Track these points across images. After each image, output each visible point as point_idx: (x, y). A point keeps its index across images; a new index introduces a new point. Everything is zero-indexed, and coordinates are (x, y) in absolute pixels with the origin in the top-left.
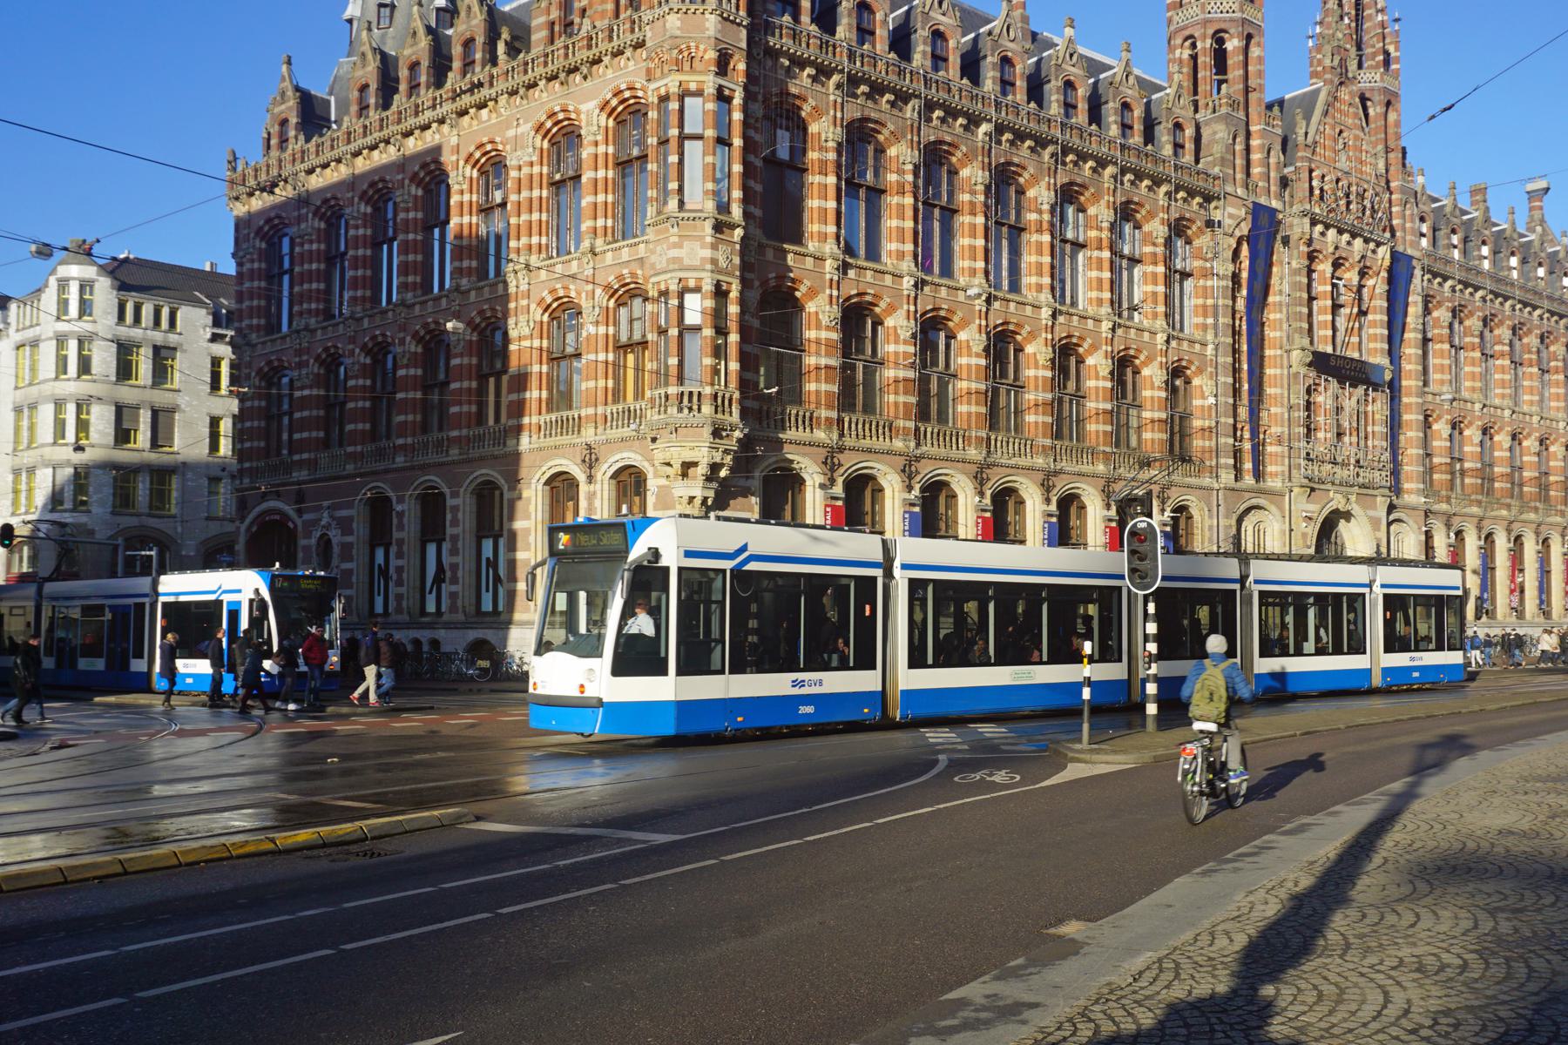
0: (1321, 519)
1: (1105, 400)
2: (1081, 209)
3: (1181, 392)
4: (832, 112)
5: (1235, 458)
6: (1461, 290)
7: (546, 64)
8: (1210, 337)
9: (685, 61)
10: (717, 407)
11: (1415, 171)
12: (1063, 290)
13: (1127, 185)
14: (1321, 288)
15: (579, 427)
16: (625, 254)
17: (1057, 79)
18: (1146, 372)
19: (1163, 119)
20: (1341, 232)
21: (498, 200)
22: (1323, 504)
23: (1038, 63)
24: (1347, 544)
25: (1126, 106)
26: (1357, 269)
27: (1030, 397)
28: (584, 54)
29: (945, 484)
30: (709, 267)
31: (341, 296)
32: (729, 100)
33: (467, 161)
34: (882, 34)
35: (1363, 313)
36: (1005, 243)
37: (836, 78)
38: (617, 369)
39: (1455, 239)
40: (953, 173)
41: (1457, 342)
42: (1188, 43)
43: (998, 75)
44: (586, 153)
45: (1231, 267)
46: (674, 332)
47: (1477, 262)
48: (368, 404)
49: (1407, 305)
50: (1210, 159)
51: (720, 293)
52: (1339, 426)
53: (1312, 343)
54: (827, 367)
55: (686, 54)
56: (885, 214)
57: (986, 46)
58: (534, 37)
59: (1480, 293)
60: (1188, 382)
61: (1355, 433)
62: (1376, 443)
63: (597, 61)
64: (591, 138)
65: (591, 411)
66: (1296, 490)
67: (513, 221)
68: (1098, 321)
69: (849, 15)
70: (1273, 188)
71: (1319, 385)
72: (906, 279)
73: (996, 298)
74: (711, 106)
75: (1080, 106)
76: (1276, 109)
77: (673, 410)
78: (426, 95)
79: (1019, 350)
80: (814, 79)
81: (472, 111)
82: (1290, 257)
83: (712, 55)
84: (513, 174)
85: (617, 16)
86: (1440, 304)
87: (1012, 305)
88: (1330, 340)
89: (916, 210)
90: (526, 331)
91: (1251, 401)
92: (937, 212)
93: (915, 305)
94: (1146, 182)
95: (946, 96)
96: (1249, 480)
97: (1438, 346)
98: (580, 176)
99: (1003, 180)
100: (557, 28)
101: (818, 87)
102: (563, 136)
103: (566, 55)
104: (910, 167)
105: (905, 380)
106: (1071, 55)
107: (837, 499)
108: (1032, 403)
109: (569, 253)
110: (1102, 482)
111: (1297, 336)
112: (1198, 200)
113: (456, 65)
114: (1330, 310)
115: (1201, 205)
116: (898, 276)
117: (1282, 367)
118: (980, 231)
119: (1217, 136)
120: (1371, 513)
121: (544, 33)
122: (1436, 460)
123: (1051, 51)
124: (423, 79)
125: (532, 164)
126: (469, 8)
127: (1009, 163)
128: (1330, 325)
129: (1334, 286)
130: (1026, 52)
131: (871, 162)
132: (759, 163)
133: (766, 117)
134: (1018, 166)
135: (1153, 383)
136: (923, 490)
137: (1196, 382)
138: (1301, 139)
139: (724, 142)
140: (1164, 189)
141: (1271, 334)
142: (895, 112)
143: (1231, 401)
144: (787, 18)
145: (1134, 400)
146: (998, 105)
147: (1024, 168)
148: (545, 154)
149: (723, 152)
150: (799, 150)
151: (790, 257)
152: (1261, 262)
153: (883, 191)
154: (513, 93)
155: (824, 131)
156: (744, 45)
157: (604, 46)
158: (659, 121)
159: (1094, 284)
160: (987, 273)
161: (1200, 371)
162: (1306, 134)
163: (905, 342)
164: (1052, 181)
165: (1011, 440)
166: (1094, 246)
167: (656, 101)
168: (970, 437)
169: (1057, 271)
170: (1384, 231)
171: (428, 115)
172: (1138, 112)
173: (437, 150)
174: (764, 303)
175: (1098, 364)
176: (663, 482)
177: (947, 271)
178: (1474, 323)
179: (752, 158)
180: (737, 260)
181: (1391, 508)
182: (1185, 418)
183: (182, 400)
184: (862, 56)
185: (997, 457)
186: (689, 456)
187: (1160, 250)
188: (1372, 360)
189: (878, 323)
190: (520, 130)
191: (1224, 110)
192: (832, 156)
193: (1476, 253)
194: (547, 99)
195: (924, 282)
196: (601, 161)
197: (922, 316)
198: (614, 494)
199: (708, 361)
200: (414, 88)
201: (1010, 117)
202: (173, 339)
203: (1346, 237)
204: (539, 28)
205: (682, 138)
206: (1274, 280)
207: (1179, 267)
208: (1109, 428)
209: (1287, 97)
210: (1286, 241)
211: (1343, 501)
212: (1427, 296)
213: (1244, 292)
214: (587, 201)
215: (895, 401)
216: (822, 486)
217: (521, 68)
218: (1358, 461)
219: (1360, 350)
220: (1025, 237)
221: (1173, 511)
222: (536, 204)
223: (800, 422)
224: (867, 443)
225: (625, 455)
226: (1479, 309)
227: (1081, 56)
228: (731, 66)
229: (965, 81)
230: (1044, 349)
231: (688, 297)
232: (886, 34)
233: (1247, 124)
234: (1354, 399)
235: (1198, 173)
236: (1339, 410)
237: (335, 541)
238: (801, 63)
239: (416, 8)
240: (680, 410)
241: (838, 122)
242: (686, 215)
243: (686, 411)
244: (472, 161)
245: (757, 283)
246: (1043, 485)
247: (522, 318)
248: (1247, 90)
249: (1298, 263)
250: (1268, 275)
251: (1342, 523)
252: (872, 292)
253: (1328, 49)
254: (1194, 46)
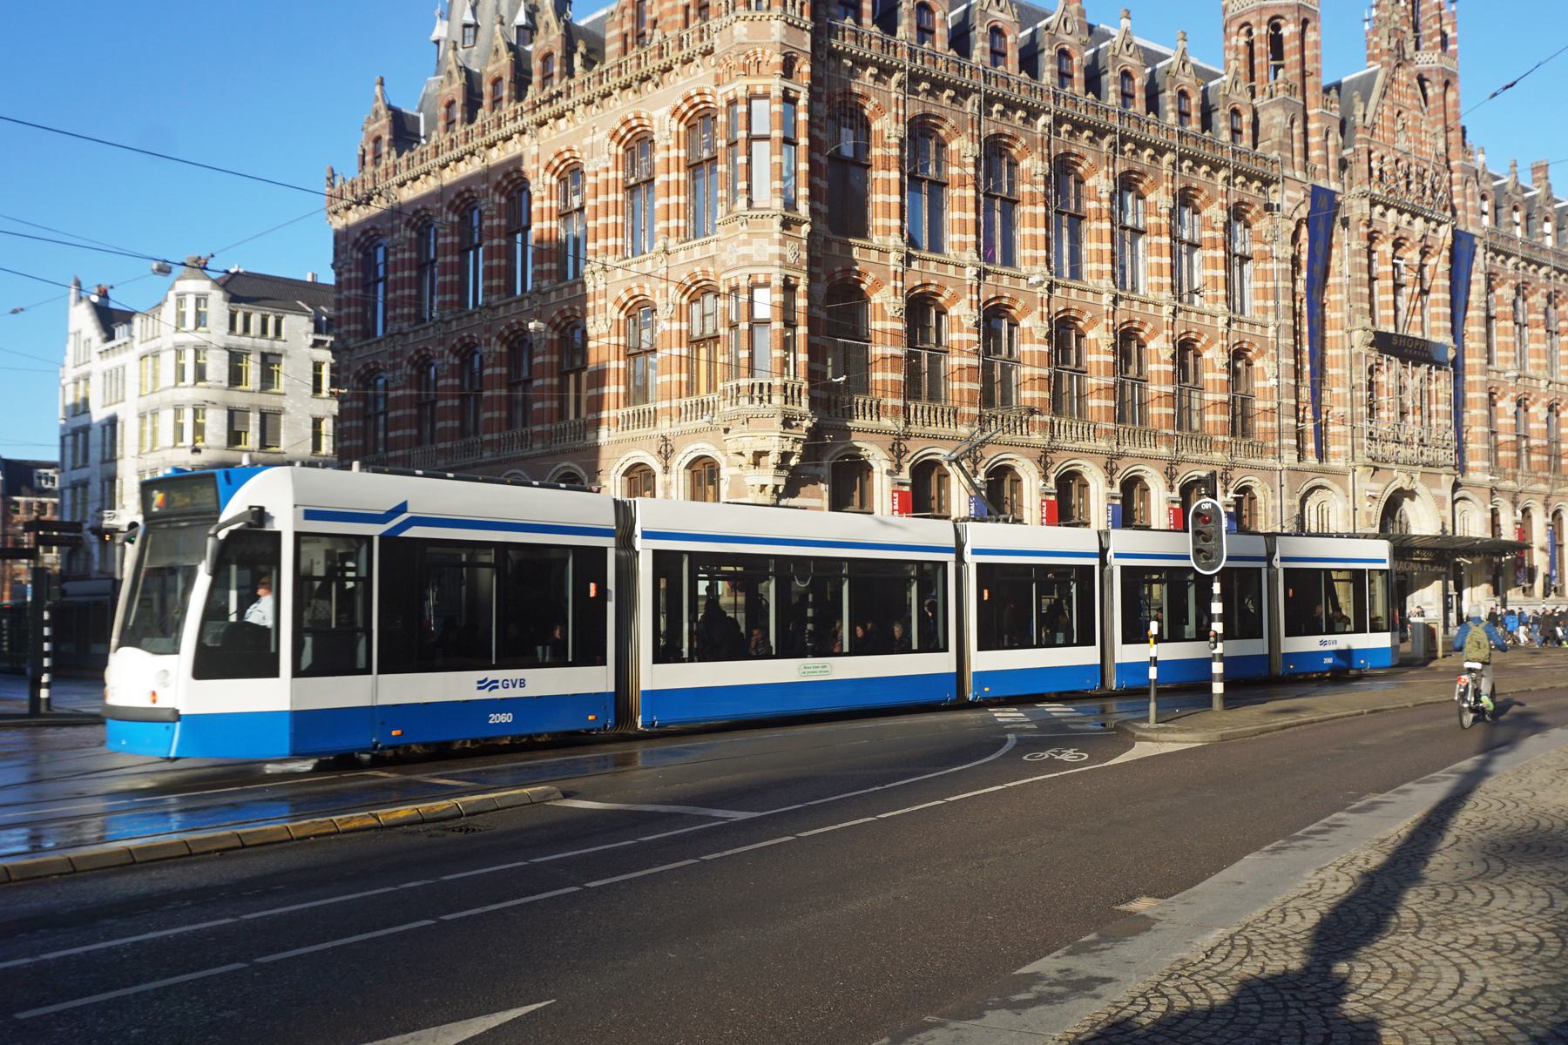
0: (1385, 498)
1: (1166, 383)
2: (1141, 196)
3: (1243, 374)
4: (894, 110)
5: (1298, 438)
6: (1524, 268)
7: (620, 74)
8: (1271, 319)
9: (751, 66)
10: (786, 397)
11: (1475, 149)
12: (1123, 276)
13: (1185, 171)
14: (1382, 268)
15: (655, 419)
16: (697, 253)
17: (1114, 69)
18: (1207, 355)
19: (1221, 106)
20: (1401, 212)
21: (577, 205)
22: (1387, 483)
23: (1096, 54)
24: (1412, 523)
25: (1183, 94)
26: (1418, 249)
27: (1092, 382)
28: (656, 63)
29: (1009, 469)
30: (777, 262)
31: (431, 301)
32: (794, 101)
33: (546, 169)
34: (941, 32)
35: (1424, 292)
36: (1065, 231)
37: (897, 76)
38: (690, 363)
39: (1517, 217)
40: (1013, 164)
41: (1521, 319)
42: (1244, 30)
43: (1056, 67)
44: (659, 157)
45: (1290, 250)
46: (744, 326)
47: (1540, 239)
48: (457, 402)
49: (1469, 283)
50: (1268, 143)
51: (788, 288)
52: (1402, 405)
53: (1373, 323)
54: (893, 356)
55: (752, 59)
56: (947, 207)
57: (1044, 40)
58: (608, 49)
59: (1544, 270)
60: (1249, 364)
61: (1418, 412)
62: (1440, 421)
63: (668, 69)
64: (664, 143)
65: (666, 404)
66: (1360, 469)
67: (591, 224)
68: (1158, 305)
69: (910, 15)
70: (1332, 171)
71: (1381, 364)
72: (969, 269)
73: (1057, 285)
74: (777, 108)
75: (1137, 95)
76: (1333, 92)
77: (744, 401)
78: (508, 108)
79: (1081, 336)
80: (877, 78)
81: (551, 121)
82: (1350, 238)
83: (778, 59)
84: (590, 180)
85: (687, 26)
86: (1503, 282)
87: (1073, 292)
88: (1392, 319)
89: (977, 202)
90: (604, 329)
91: (1313, 382)
92: (998, 203)
93: (978, 294)
94: (1205, 168)
95: (1005, 90)
96: (1311, 460)
97: (1502, 324)
98: (653, 180)
99: (1063, 171)
100: (629, 40)
101: (880, 86)
102: (637, 143)
103: (639, 65)
104: (971, 160)
105: (969, 367)
106: (1128, 46)
107: (904, 484)
108: (1094, 388)
109: (644, 253)
110: (1165, 464)
111: (1358, 316)
112: (1257, 184)
113: (536, 78)
114: (1391, 290)
115: (1259, 189)
116: (960, 267)
117: (1343, 348)
118: (1041, 220)
119: (1275, 121)
120: (1435, 491)
121: (618, 45)
122: (1501, 438)
123: (1107, 43)
124: (505, 93)
125: (607, 170)
126: (547, 24)
127: (1068, 154)
128: (1391, 305)
129: (1395, 265)
130: (1083, 44)
131: (932, 156)
132: (823, 161)
133: (830, 117)
134: (1077, 156)
135: (1214, 366)
136: (988, 474)
137: (1257, 364)
138: (1359, 121)
139: (789, 141)
140: (1222, 174)
141: (1330, 314)
142: (956, 107)
143: (1293, 382)
144: (849, 21)
145: (1196, 382)
146: (1056, 97)
147: (1083, 158)
148: (620, 160)
149: (790, 152)
150: (863, 147)
151: (855, 251)
152: (1320, 245)
153: (946, 185)
154: (589, 103)
155: (887, 128)
156: (808, 48)
157: (675, 55)
158: (727, 124)
159: (1155, 270)
160: (1048, 261)
161: (1261, 353)
162: (1365, 116)
163: (969, 330)
164: (1111, 170)
165: (1074, 424)
166: (1154, 231)
167: (724, 105)
168: (1034, 422)
169: (1117, 257)
170: (1445, 210)
171: (510, 127)
172: (1195, 100)
173: (518, 160)
174: (831, 296)
175: (1159, 349)
176: (736, 471)
177: (1009, 260)
178: (1538, 300)
179: (817, 156)
180: (804, 255)
181: (1456, 486)
182: (1246, 400)
183: (287, 403)
184: (923, 54)
185: (1061, 441)
186: (760, 446)
187: (1219, 235)
188: (1434, 339)
189: (942, 312)
190: (596, 138)
191: (1281, 95)
192: (895, 152)
193: (1538, 230)
194: (622, 107)
195: (986, 272)
196: (673, 164)
197: (984, 304)
198: (689, 483)
199: (778, 353)
200: (496, 102)
201: (1068, 109)
202: (278, 346)
203: (1406, 217)
204: (613, 40)
205: (750, 139)
206: (1334, 262)
207: (1238, 251)
208: (1171, 411)
209: (1344, 80)
210: (1345, 223)
211: (1407, 480)
212: (1490, 274)
213: (1304, 274)
214: (660, 202)
215: (960, 388)
216: (889, 472)
217: (597, 78)
218: (1422, 440)
219: (1423, 330)
220: (1085, 225)
221: (1236, 492)
222: (611, 208)
223: (867, 411)
224: (932, 430)
225: (699, 445)
226: (1543, 286)
227: (1138, 47)
228: (796, 69)
229: (1024, 74)
230: (1105, 334)
231: (758, 292)
232: (945, 32)
233: (1305, 108)
234: (1417, 378)
235: (1256, 158)
236: (1402, 389)
238: (863, 63)
239: (498, 27)
240: (752, 400)
241: (901, 119)
242: (754, 213)
243: (757, 401)
244: (552, 169)
245: (824, 277)
246: (1106, 468)
247: (601, 317)
248: (1304, 75)
249: (1359, 244)
250: (1328, 256)
251: (1407, 500)
252: (936, 282)
253: (1384, 32)
254: (1250, 33)
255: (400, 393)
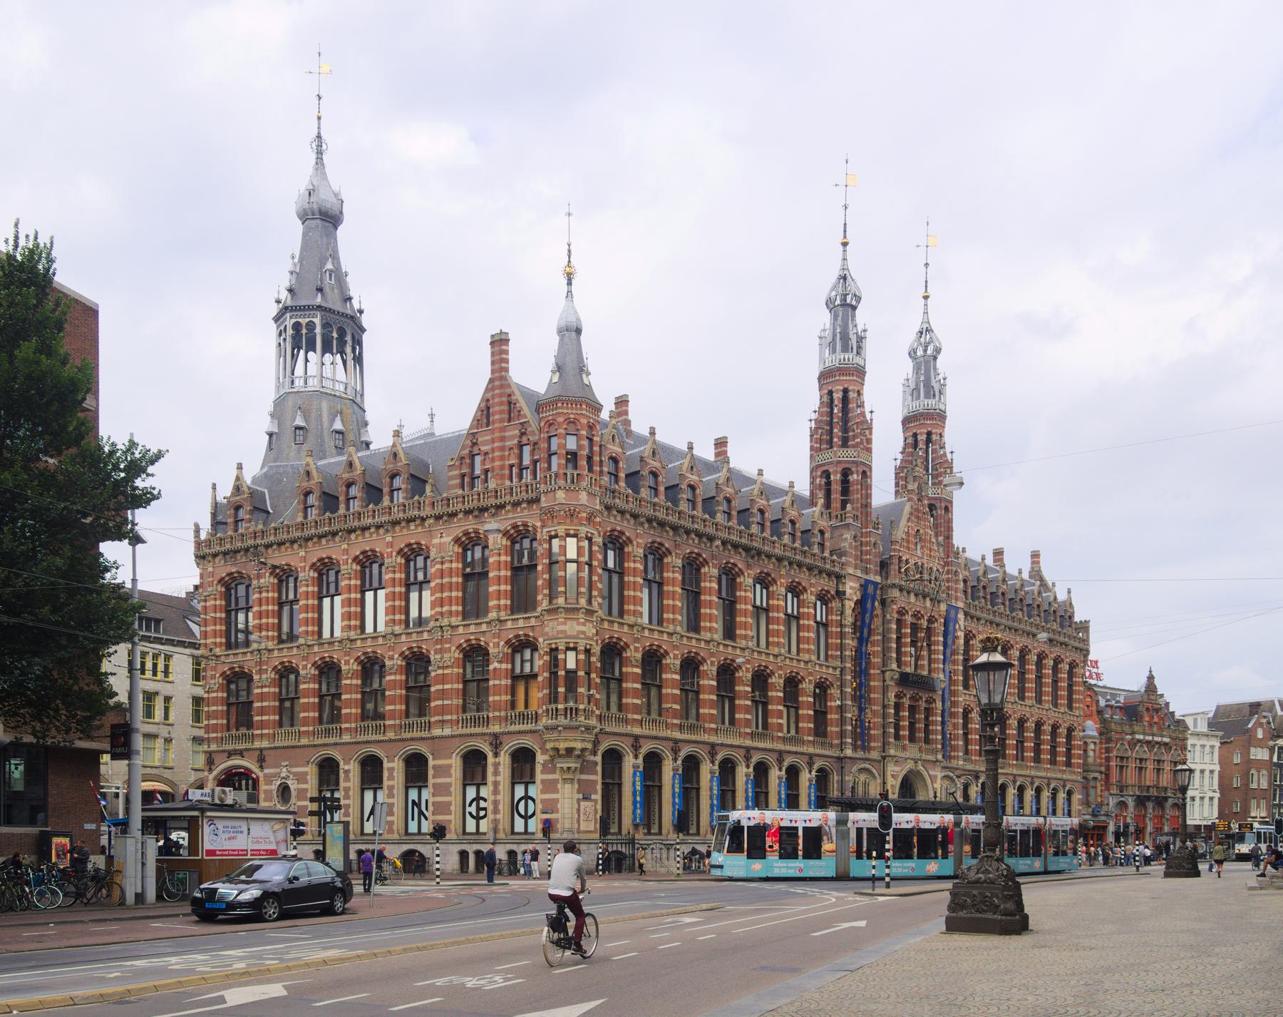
190: (443, 540)
237: (292, 787)
240: (566, 718)
255: (265, 690)
